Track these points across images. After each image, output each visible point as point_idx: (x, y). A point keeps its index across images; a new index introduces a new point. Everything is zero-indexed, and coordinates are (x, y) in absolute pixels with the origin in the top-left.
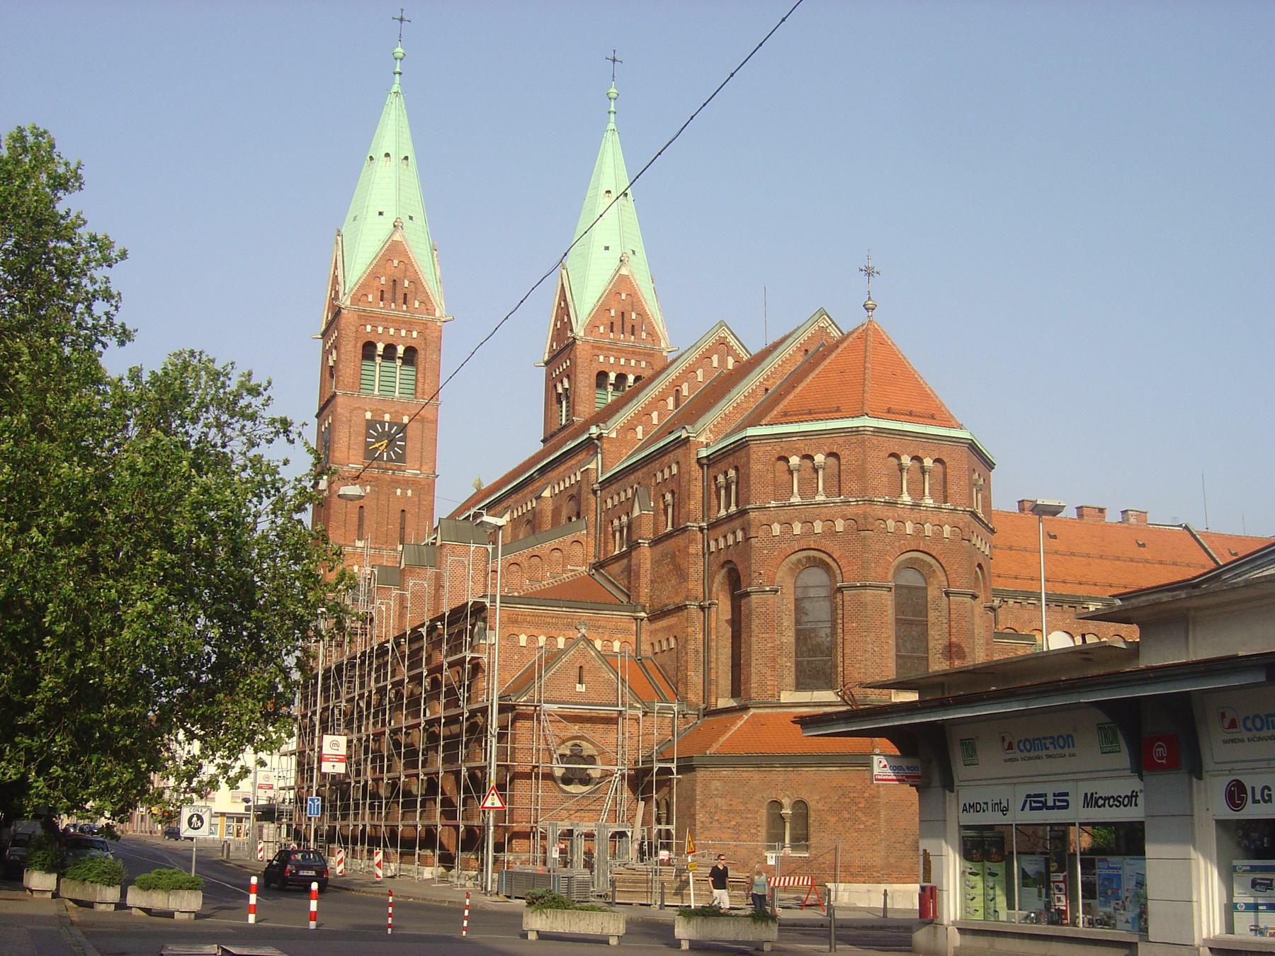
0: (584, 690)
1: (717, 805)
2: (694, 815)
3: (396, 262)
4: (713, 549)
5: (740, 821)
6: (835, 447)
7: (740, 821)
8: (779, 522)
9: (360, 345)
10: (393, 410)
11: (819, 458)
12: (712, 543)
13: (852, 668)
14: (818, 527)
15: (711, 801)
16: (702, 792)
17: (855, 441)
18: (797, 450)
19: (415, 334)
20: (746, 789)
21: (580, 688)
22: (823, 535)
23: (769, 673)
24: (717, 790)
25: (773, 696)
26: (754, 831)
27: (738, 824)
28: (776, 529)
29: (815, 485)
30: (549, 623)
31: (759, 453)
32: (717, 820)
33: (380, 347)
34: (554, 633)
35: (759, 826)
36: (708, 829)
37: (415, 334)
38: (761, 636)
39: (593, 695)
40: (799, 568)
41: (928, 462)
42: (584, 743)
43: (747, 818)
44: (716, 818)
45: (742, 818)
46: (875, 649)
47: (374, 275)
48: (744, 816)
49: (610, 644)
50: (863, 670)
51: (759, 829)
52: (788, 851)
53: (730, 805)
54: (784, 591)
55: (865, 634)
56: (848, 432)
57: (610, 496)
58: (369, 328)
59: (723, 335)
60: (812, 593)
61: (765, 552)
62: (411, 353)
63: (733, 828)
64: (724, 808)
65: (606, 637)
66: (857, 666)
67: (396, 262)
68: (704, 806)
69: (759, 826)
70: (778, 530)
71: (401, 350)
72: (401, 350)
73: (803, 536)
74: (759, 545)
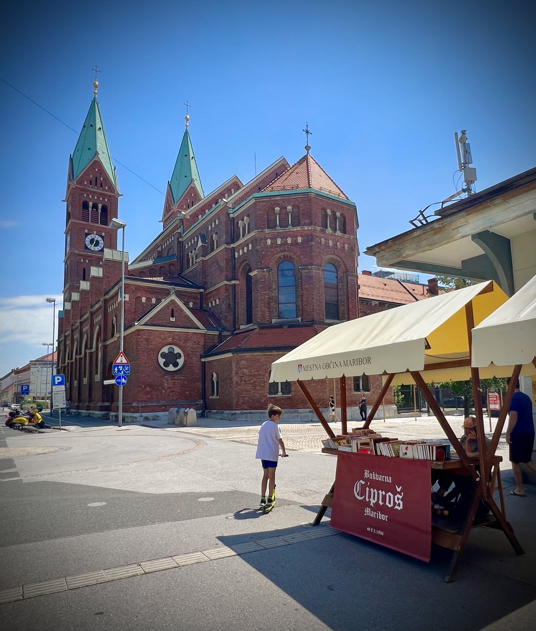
0: (174, 321)
1: (244, 372)
2: (232, 378)
3: (97, 170)
4: (236, 256)
5: (255, 380)
6: (297, 202)
7: (255, 380)
8: (270, 239)
9: (82, 201)
10: (97, 230)
11: (289, 208)
12: (236, 254)
13: (307, 307)
14: (289, 240)
15: (241, 370)
16: (236, 366)
17: (307, 200)
18: (279, 204)
19: (106, 200)
20: (258, 364)
21: (173, 319)
22: (292, 244)
23: (266, 310)
24: (244, 365)
25: (268, 321)
26: (262, 385)
27: (255, 382)
28: (269, 242)
29: (287, 222)
30: (157, 292)
31: (260, 206)
32: (244, 380)
33: (91, 204)
34: (160, 297)
35: (265, 382)
36: (239, 385)
37: (106, 200)
38: (262, 292)
39: (179, 323)
40: (280, 261)
41: (338, 214)
42: (175, 347)
43: (259, 378)
44: (243, 379)
45: (256, 379)
46: (317, 298)
47: (87, 173)
48: (258, 377)
49: (188, 304)
50: (312, 308)
51: (265, 383)
52: (280, 394)
53: (250, 372)
54: (273, 271)
55: (313, 290)
56: (303, 195)
57: (187, 243)
58: (85, 195)
59: (236, 181)
60: (286, 272)
61: (264, 253)
62: (104, 209)
63: (252, 384)
64: (248, 374)
65: (186, 300)
66: (309, 305)
67: (97, 170)
68: (237, 373)
69: (265, 382)
70: (270, 242)
71: (100, 206)
72: (100, 206)
73: (282, 245)
74: (260, 250)
